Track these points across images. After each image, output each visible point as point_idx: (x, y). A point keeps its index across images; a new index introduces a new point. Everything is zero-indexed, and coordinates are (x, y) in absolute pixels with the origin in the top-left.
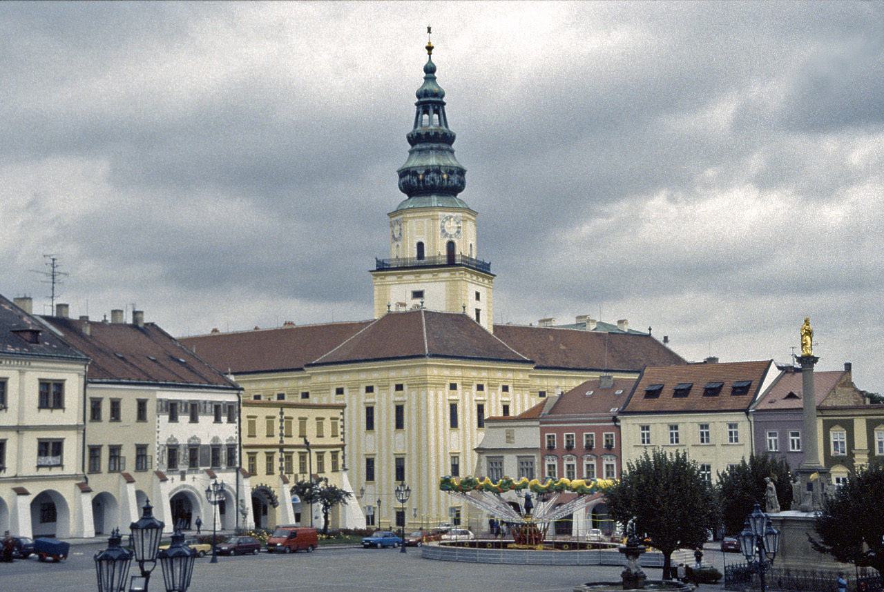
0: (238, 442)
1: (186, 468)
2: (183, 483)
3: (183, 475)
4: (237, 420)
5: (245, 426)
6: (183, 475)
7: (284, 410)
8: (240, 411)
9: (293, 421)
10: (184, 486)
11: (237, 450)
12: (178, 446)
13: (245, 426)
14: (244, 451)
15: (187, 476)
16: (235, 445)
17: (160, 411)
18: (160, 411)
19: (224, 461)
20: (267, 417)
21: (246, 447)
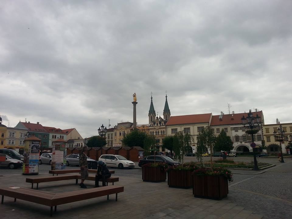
0: (262, 134)
1: (242, 141)
2: (241, 144)
3: (241, 142)
4: (261, 129)
5: (264, 131)
6: (241, 142)
7: (282, 125)
8: (262, 127)
9: (287, 128)
10: (242, 144)
11: (262, 136)
12: (238, 137)
13: (264, 131)
14: (264, 137)
15: (243, 143)
16: (261, 135)
17: (231, 130)
18: (231, 130)
19: (256, 138)
20: (274, 128)
21: (264, 135)
